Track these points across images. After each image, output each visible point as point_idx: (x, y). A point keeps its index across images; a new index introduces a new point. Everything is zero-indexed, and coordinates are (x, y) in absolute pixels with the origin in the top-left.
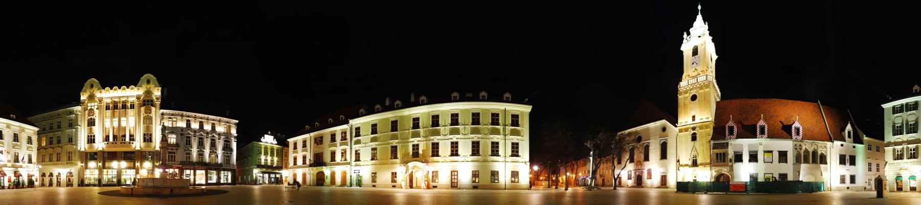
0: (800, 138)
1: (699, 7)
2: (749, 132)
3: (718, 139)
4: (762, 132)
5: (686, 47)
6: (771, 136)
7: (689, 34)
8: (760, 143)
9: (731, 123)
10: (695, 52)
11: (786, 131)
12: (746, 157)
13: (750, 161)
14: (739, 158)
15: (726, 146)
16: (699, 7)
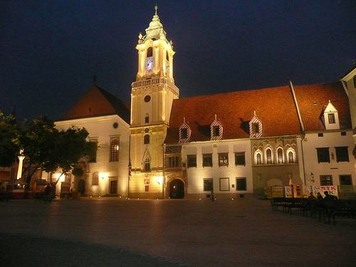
0: (258, 136)
1: (156, 8)
2: (203, 133)
3: (170, 143)
4: (217, 133)
5: (142, 48)
6: (227, 136)
7: (144, 34)
8: (214, 145)
9: (184, 126)
10: (150, 53)
11: (242, 129)
12: (200, 161)
13: (204, 165)
14: (192, 162)
15: (178, 149)
16: (156, 8)
